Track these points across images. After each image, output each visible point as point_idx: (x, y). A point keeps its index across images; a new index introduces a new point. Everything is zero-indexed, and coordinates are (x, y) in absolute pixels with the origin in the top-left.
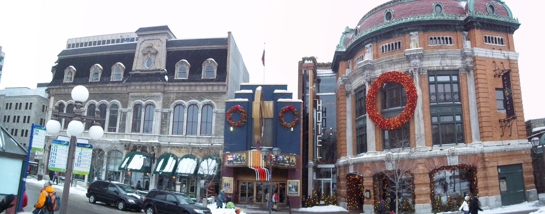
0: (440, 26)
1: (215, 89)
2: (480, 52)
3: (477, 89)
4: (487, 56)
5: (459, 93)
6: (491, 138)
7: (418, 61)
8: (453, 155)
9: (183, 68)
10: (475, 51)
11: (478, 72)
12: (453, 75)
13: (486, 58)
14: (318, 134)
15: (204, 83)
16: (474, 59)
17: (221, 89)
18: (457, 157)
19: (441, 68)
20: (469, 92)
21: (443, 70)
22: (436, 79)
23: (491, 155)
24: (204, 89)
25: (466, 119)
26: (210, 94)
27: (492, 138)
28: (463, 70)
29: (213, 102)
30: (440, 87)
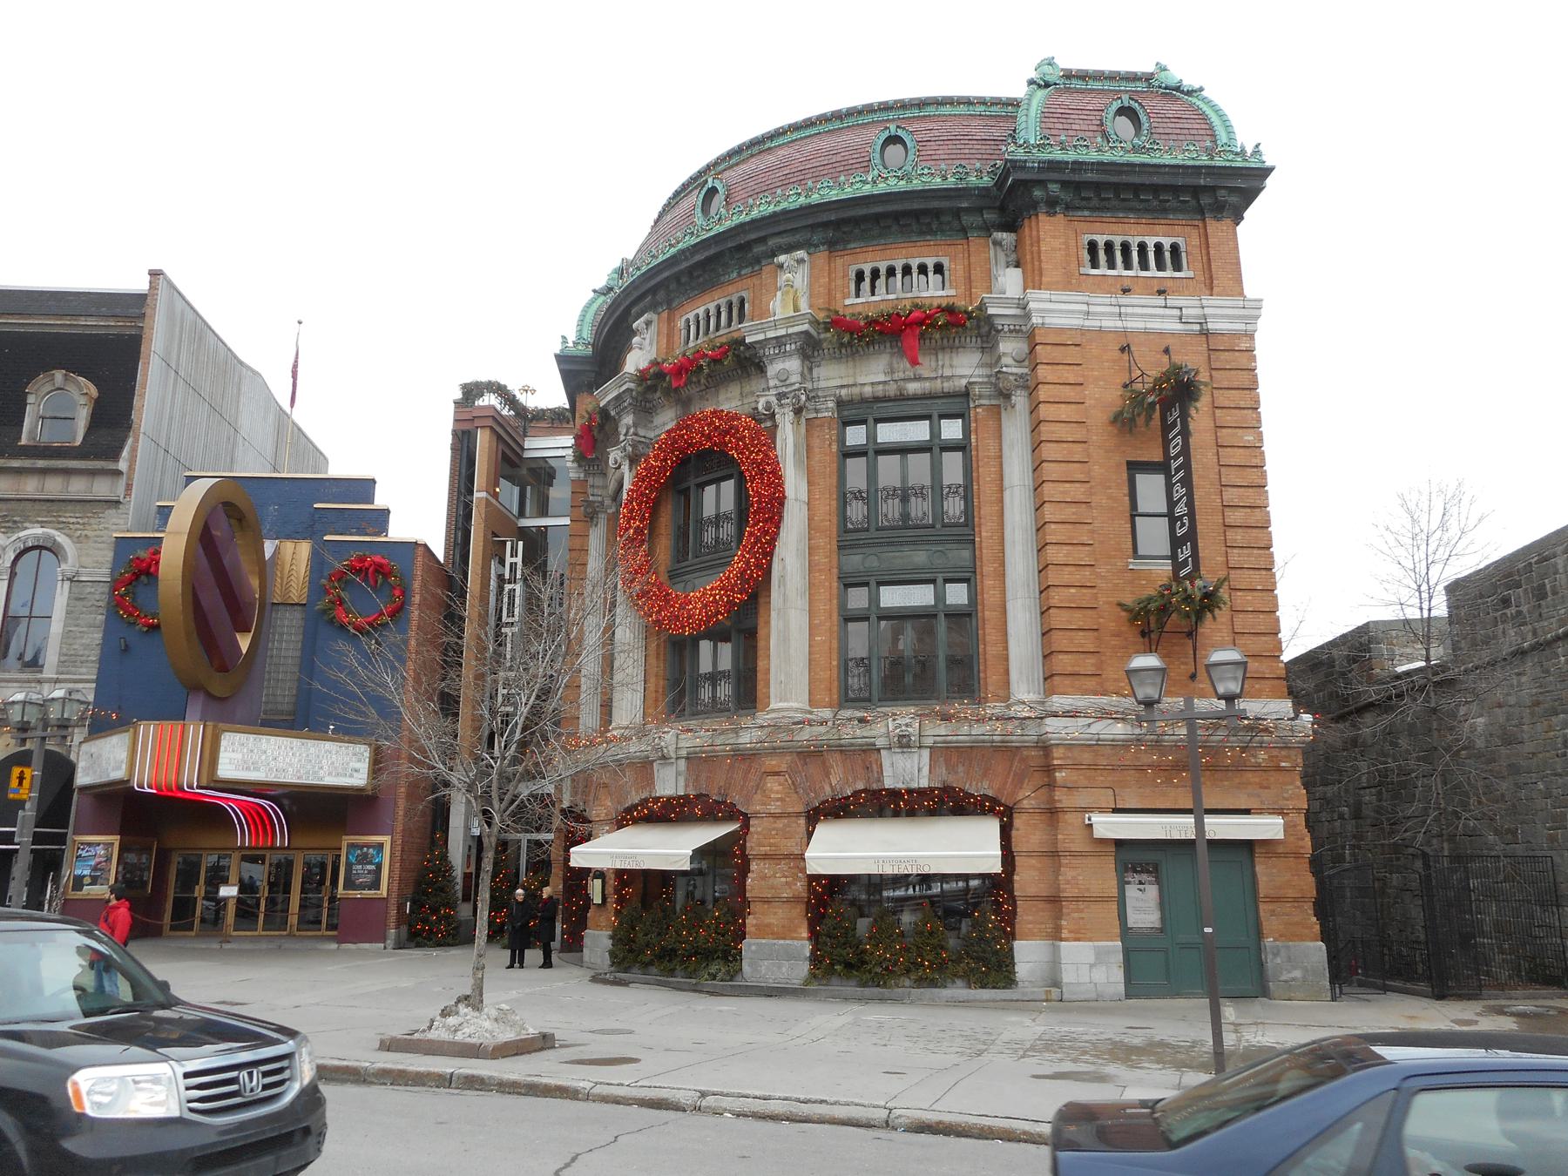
0: (897, 216)
1: (78, 487)
2: (1057, 309)
4: (1092, 323)
5: (967, 492)
6: (1091, 683)
8: (904, 743)
10: (1032, 305)
11: (1043, 393)
12: (942, 416)
13: (1082, 331)
15: (27, 463)
17: (102, 488)
18: (926, 753)
19: (892, 390)
20: (1006, 483)
21: (902, 398)
22: (872, 436)
23: (1087, 757)
25: (989, 596)
26: (52, 506)
28: (986, 391)
29: (61, 538)
30: (889, 469)
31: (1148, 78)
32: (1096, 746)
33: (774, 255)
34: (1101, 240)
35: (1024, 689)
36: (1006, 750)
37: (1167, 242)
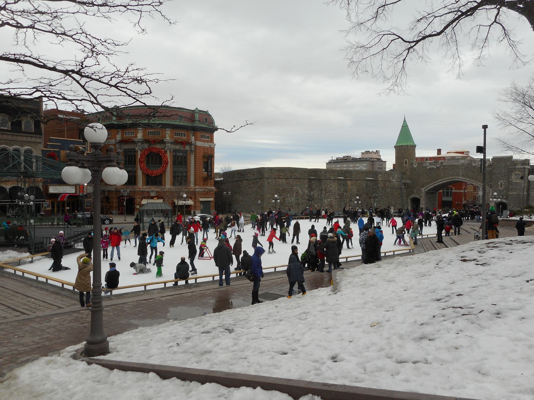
1: (33, 140)
2: (199, 143)
3: (195, 161)
7: (170, 145)
15: (24, 135)
16: (196, 146)
17: (38, 140)
24: (25, 139)
27: (199, 185)
32: (200, 191)
33: (165, 128)
35: (192, 185)
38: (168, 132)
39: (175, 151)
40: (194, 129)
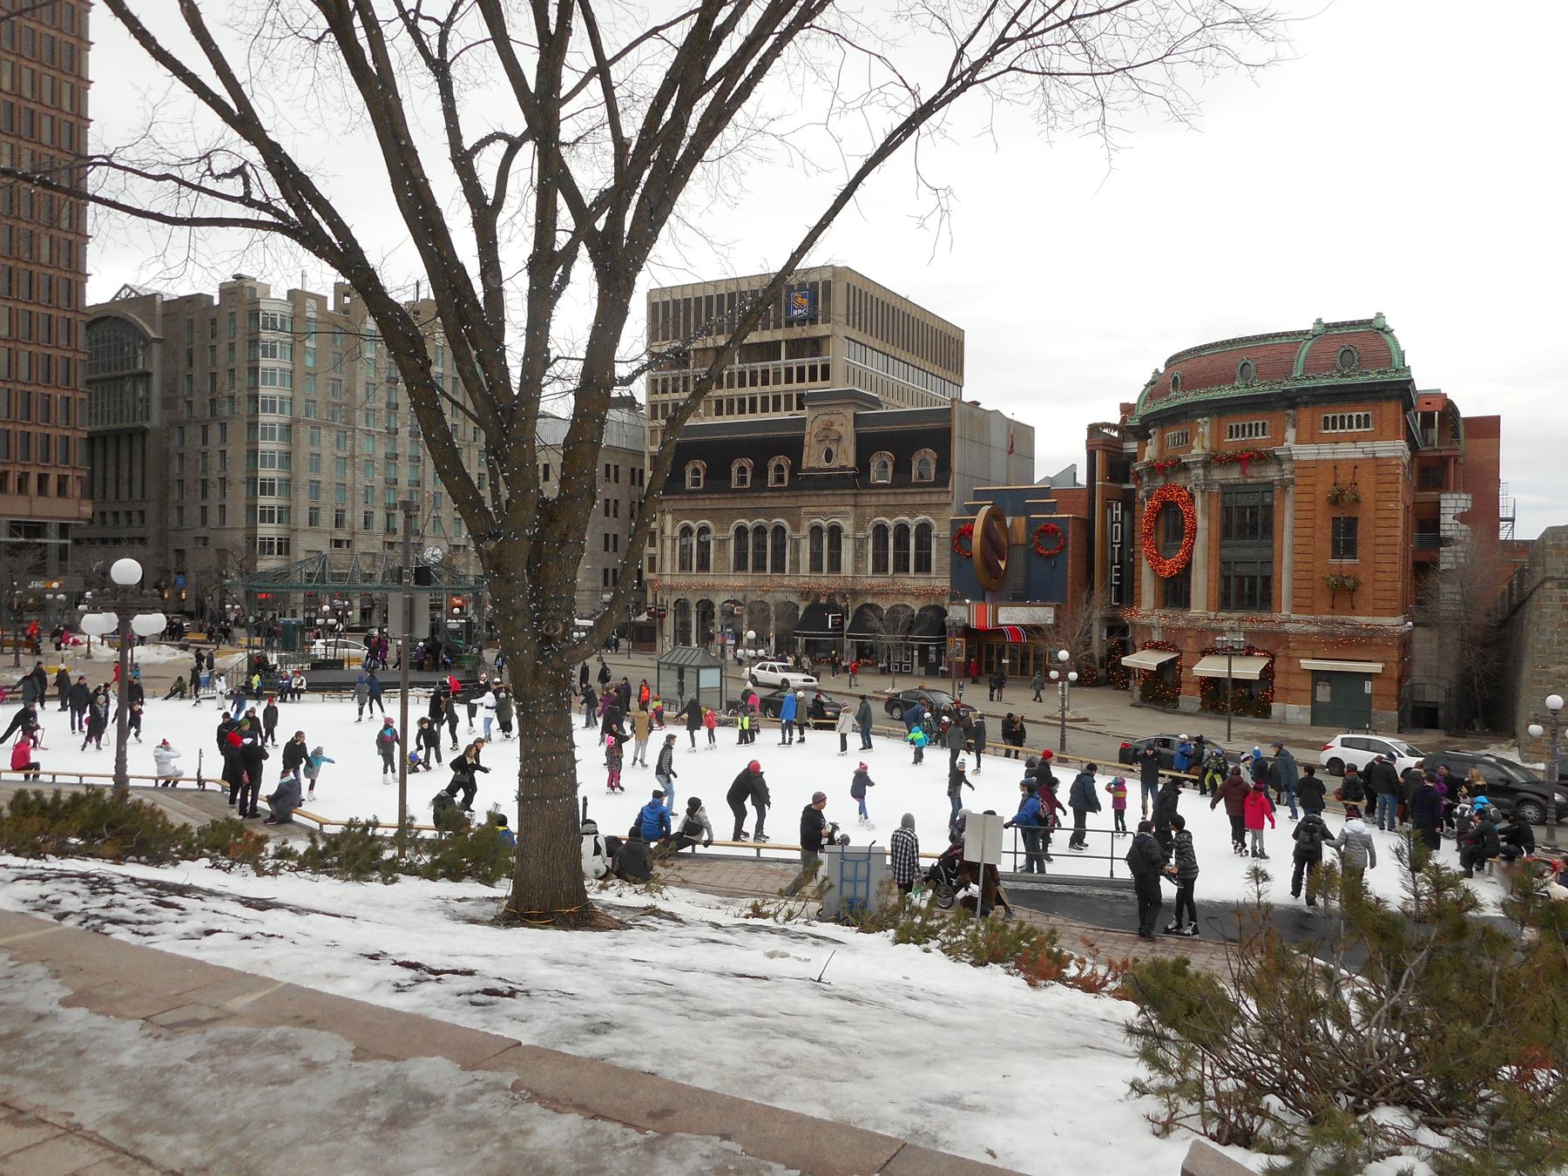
1: (934, 499)
9: (881, 468)
14: (1113, 563)
17: (943, 499)
21: (1246, 484)
24: (918, 499)
31: (1370, 321)
32: (1307, 634)
34: (1330, 416)
36: (1274, 634)
37: (1362, 414)
38: (1204, 427)
39: (1227, 489)
40: (1290, 401)
